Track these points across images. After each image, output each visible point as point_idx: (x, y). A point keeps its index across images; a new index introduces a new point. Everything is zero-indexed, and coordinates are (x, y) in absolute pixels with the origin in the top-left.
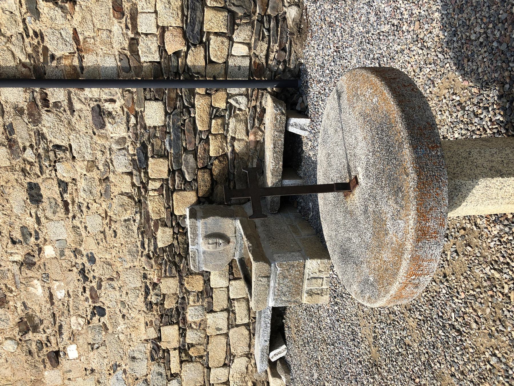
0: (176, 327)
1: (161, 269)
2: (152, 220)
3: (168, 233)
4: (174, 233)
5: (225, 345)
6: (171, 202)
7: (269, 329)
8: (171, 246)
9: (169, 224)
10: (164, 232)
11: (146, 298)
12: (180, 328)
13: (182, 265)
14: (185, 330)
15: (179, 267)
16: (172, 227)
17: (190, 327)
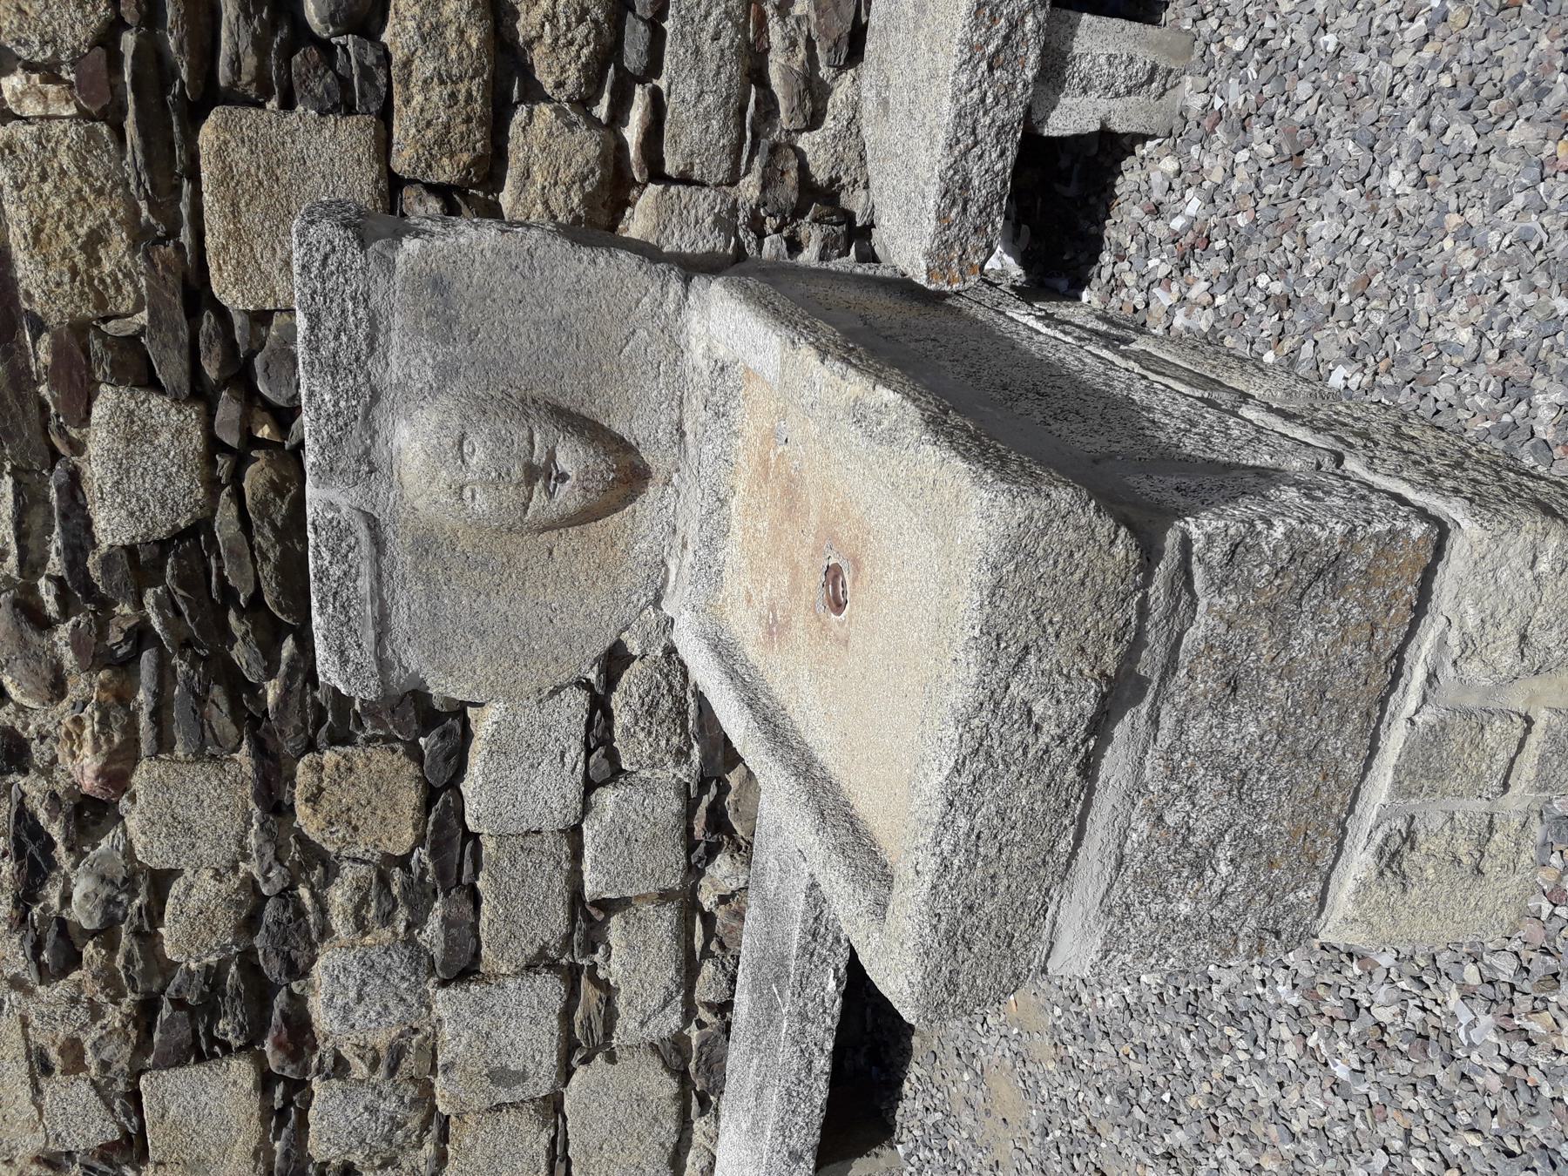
0: (241, 1071)
1: (123, 698)
2: (38, 326)
3: (164, 438)
4: (214, 445)
5: (543, 1162)
6: (186, 187)
7: (822, 1085)
8: (194, 536)
9: (172, 369)
10: (134, 433)
11: (26, 896)
12: (266, 1081)
13: (272, 690)
14: (299, 1086)
15: (255, 691)
16: (200, 393)
17: (340, 1067)
